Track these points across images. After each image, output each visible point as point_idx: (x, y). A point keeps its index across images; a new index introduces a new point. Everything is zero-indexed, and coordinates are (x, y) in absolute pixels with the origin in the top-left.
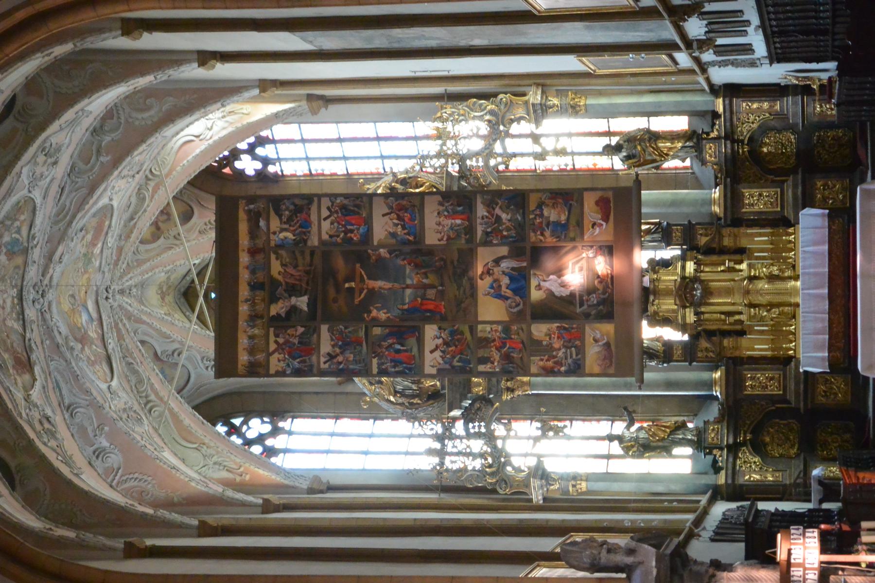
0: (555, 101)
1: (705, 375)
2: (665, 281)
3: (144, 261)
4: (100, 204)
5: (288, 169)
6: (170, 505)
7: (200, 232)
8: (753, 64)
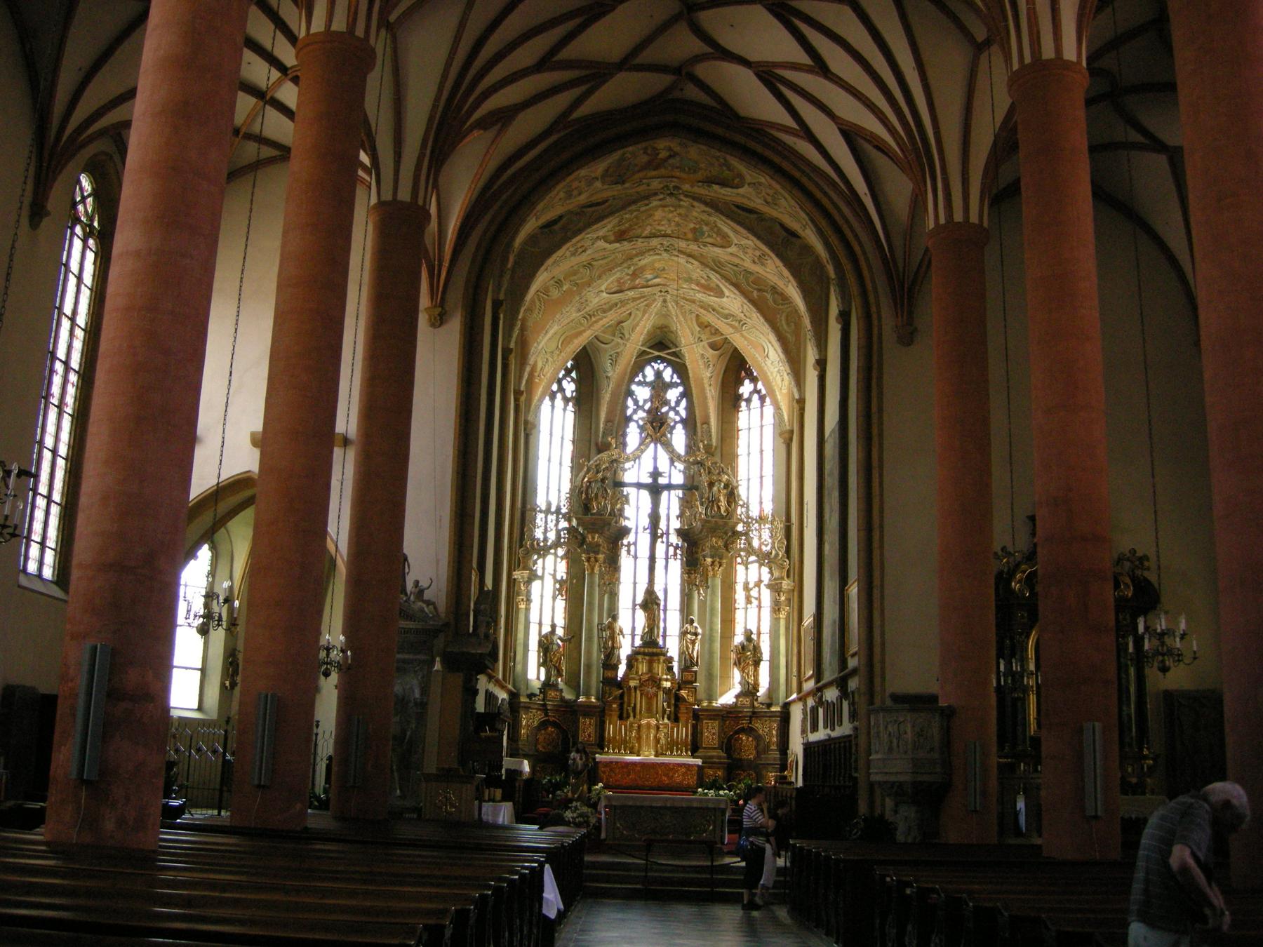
0: (783, 598)
1: (593, 691)
3: (684, 317)
4: (725, 290)
6: (523, 329)
8: (804, 732)
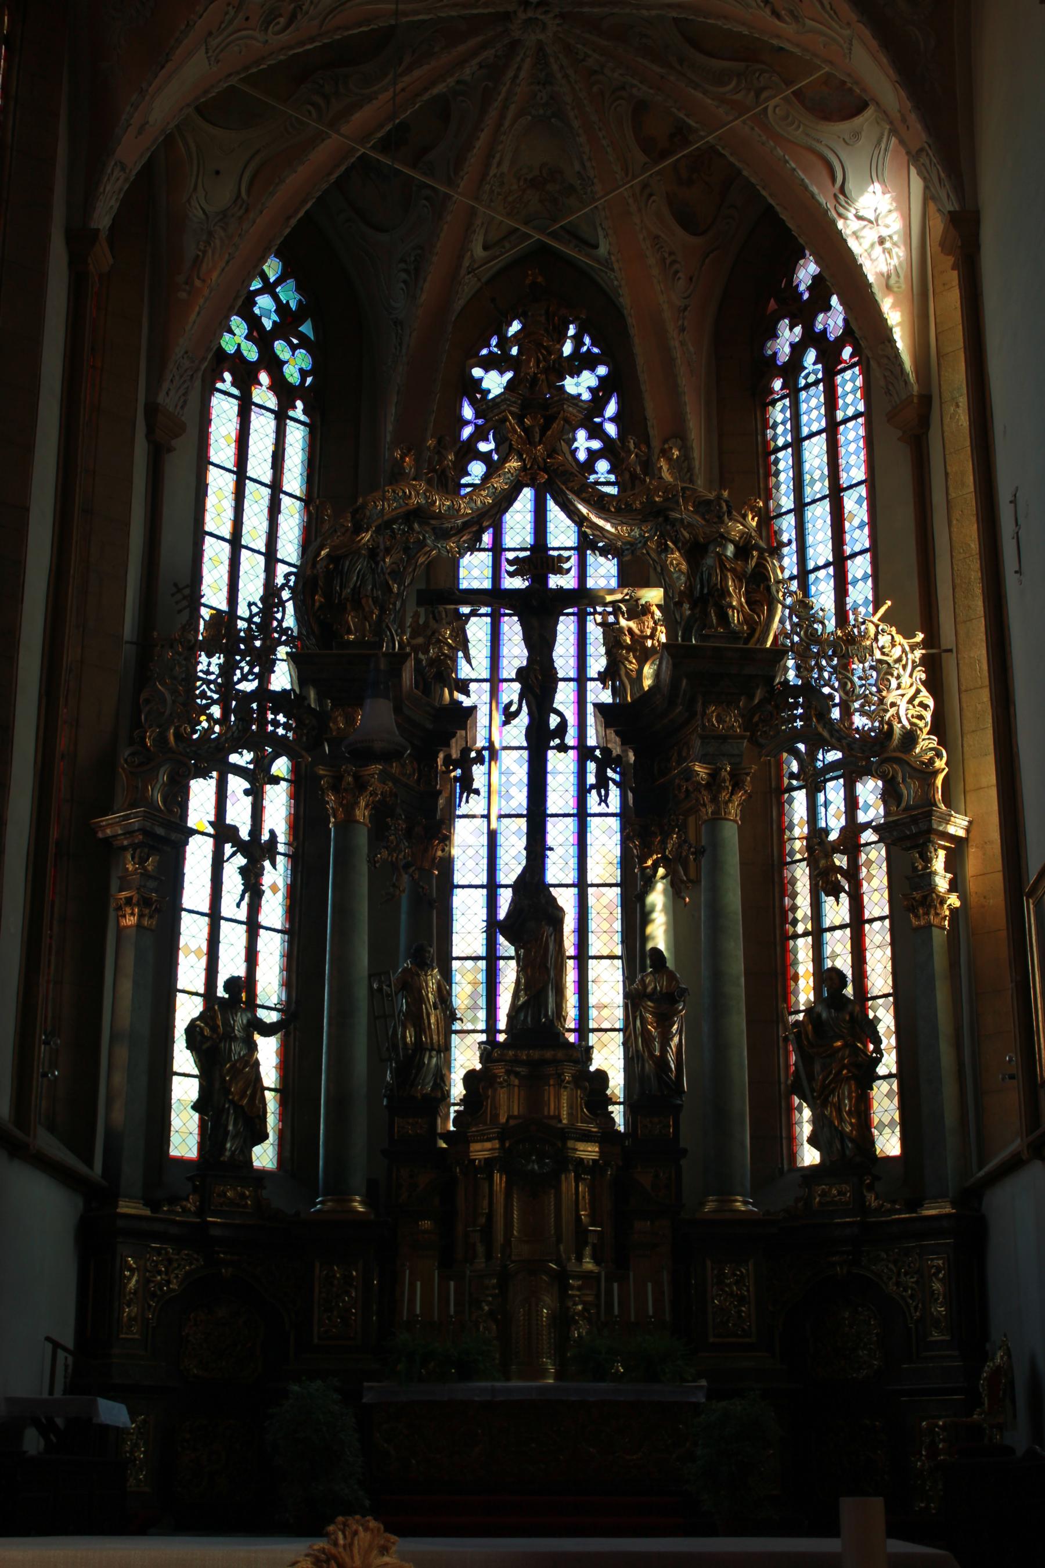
2: (558, 1097)
5: (779, 413)
7: (657, 237)
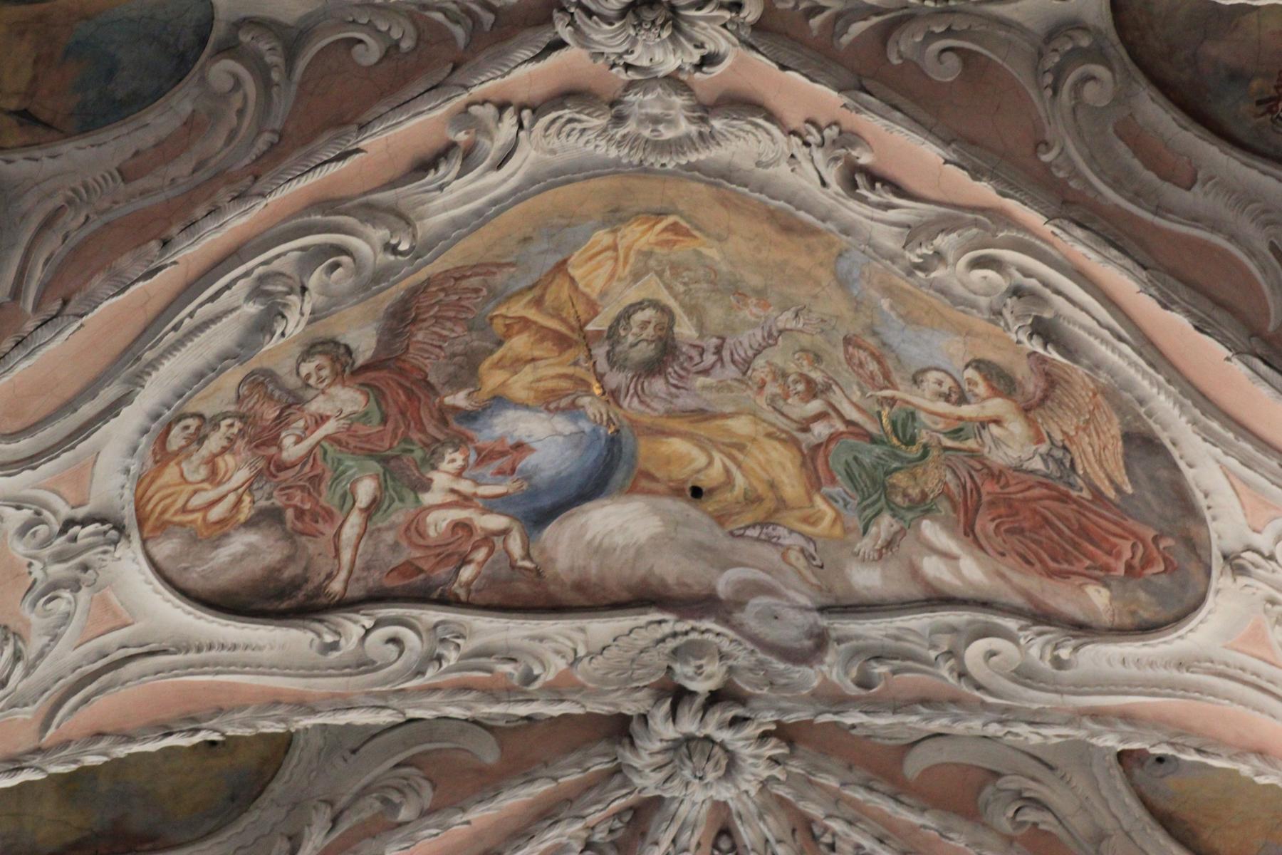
4: (1207, 468)
